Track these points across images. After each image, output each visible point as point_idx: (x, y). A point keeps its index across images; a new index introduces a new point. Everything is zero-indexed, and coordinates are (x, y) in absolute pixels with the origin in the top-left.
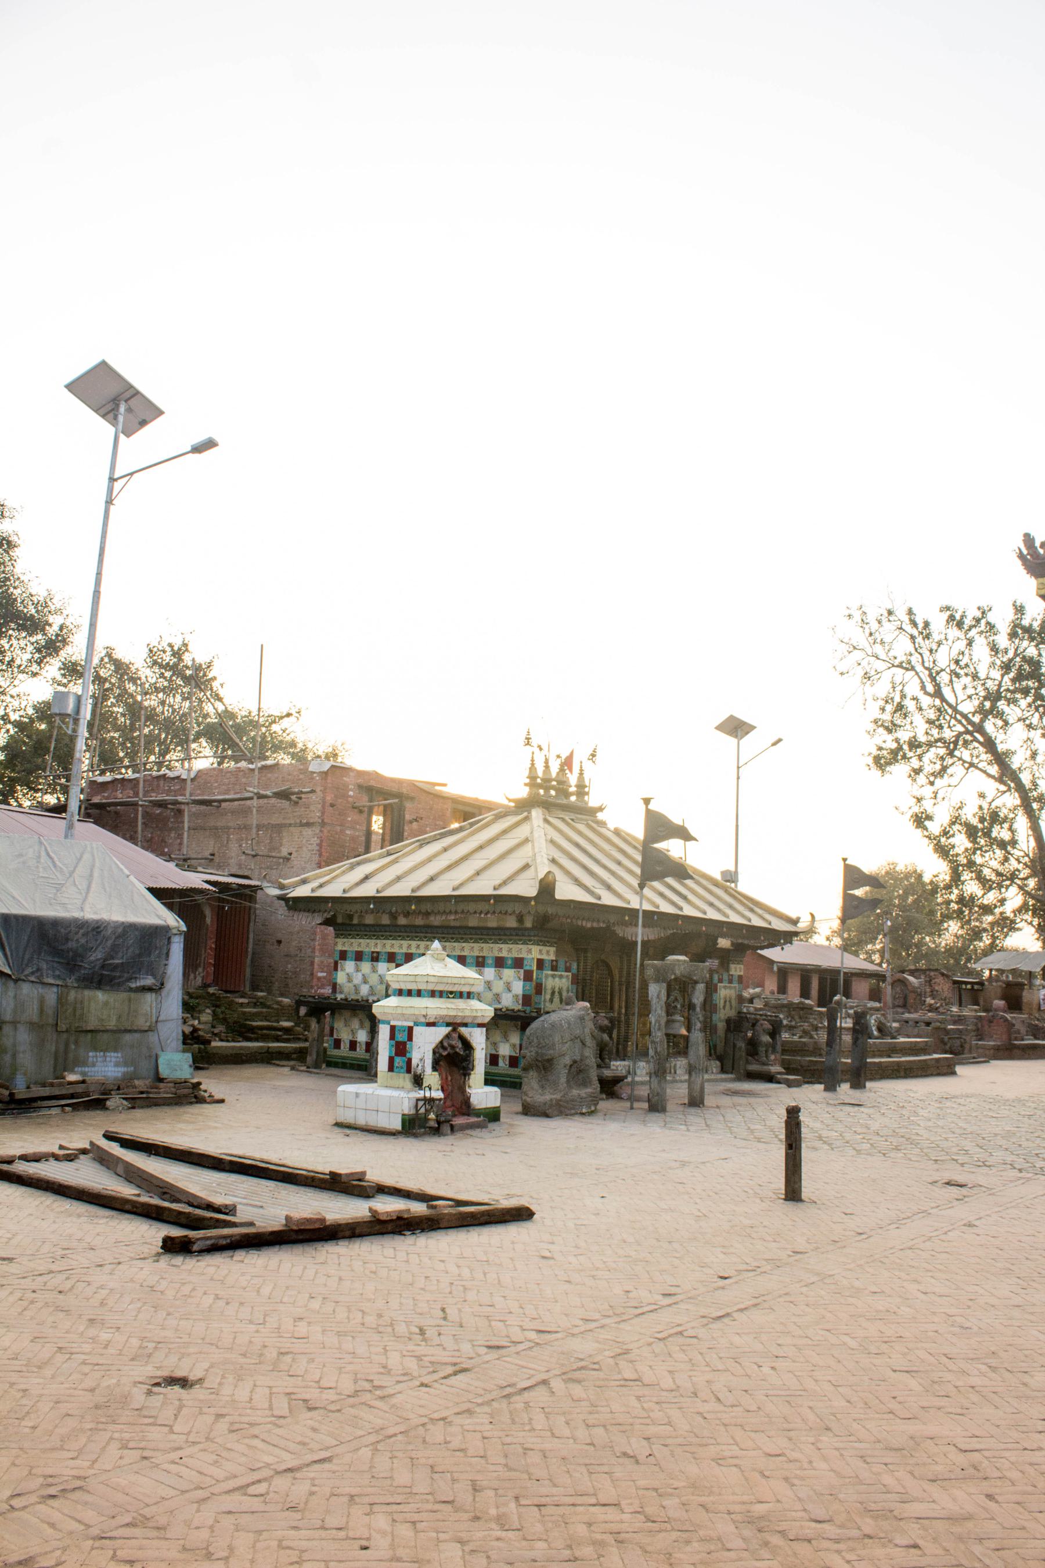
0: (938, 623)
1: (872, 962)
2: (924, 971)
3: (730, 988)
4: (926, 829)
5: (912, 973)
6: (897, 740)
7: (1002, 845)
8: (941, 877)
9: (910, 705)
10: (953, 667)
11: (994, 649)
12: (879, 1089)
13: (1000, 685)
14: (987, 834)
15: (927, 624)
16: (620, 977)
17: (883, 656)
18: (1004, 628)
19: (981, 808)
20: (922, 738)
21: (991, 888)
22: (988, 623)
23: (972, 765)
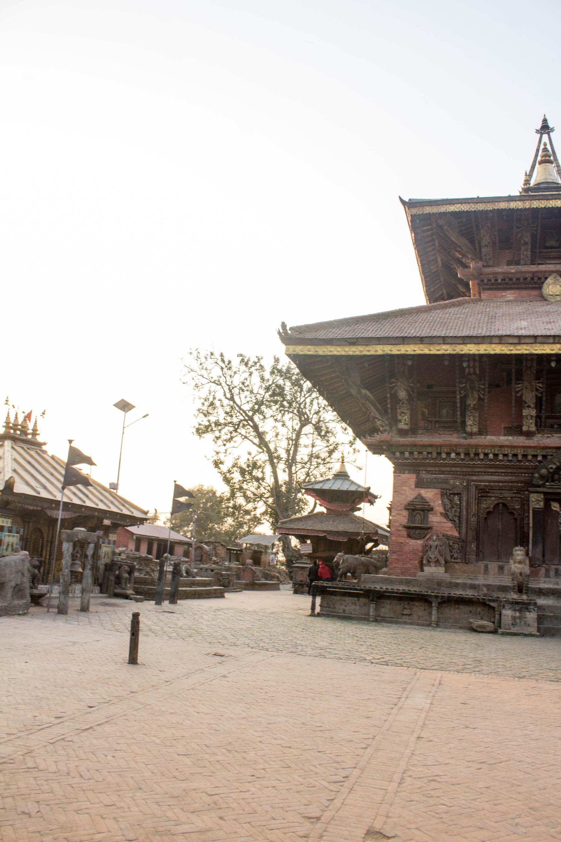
0: (236, 362)
1: (186, 537)
2: (212, 543)
3: (109, 547)
4: (220, 469)
5: (206, 543)
6: (209, 421)
7: (257, 479)
8: (225, 494)
9: (217, 403)
10: (241, 386)
11: (262, 379)
12: (184, 604)
13: (263, 398)
14: (250, 474)
15: (230, 362)
16: (48, 538)
17: (206, 376)
18: (268, 369)
19: (248, 460)
20: (222, 421)
21: (250, 502)
22: (261, 365)
23: (246, 437)
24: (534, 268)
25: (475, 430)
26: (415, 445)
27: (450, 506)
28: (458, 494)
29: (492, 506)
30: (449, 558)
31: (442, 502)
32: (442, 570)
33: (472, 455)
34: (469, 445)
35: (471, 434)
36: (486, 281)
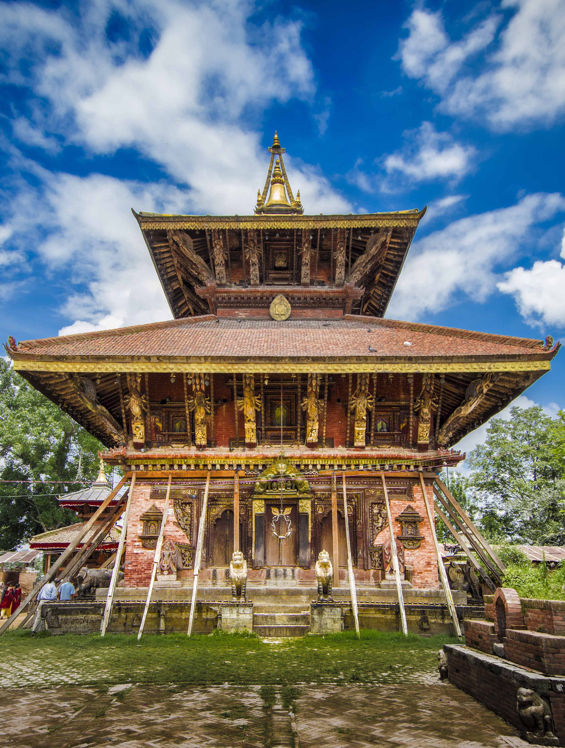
24: (261, 288)
25: (204, 442)
26: (149, 458)
27: (182, 515)
28: (189, 503)
29: (220, 514)
30: (181, 566)
31: (175, 511)
32: (174, 577)
33: (201, 467)
34: (198, 457)
35: (200, 447)
36: (220, 299)
